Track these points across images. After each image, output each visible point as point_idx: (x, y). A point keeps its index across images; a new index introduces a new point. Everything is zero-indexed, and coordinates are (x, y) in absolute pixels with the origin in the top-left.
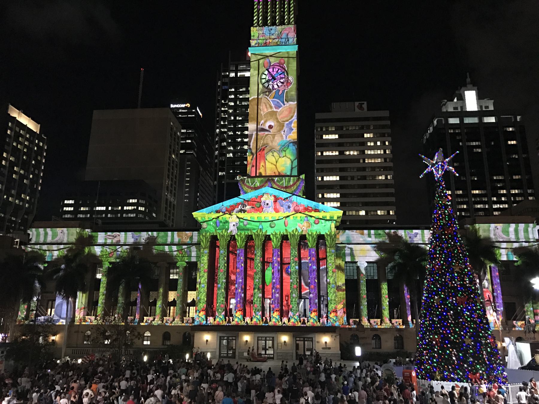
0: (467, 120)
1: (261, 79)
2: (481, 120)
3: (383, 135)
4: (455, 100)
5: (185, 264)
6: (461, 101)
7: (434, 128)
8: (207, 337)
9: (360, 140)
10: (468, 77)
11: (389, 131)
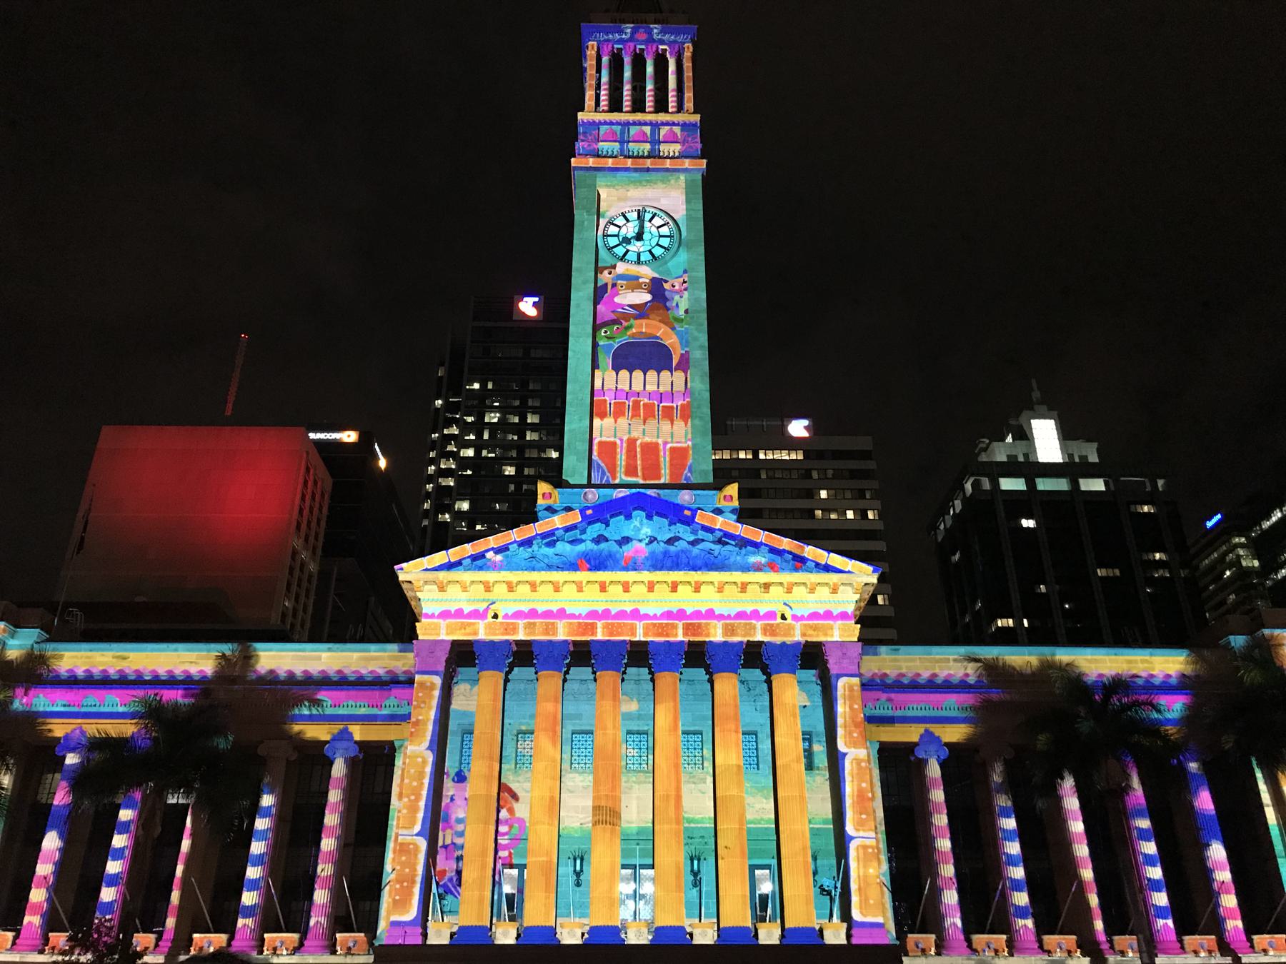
0: (1043, 484)
2: (1075, 484)
3: (861, 494)
4: (1009, 439)
6: (1024, 442)
7: (965, 501)
9: (803, 504)
11: (875, 484)
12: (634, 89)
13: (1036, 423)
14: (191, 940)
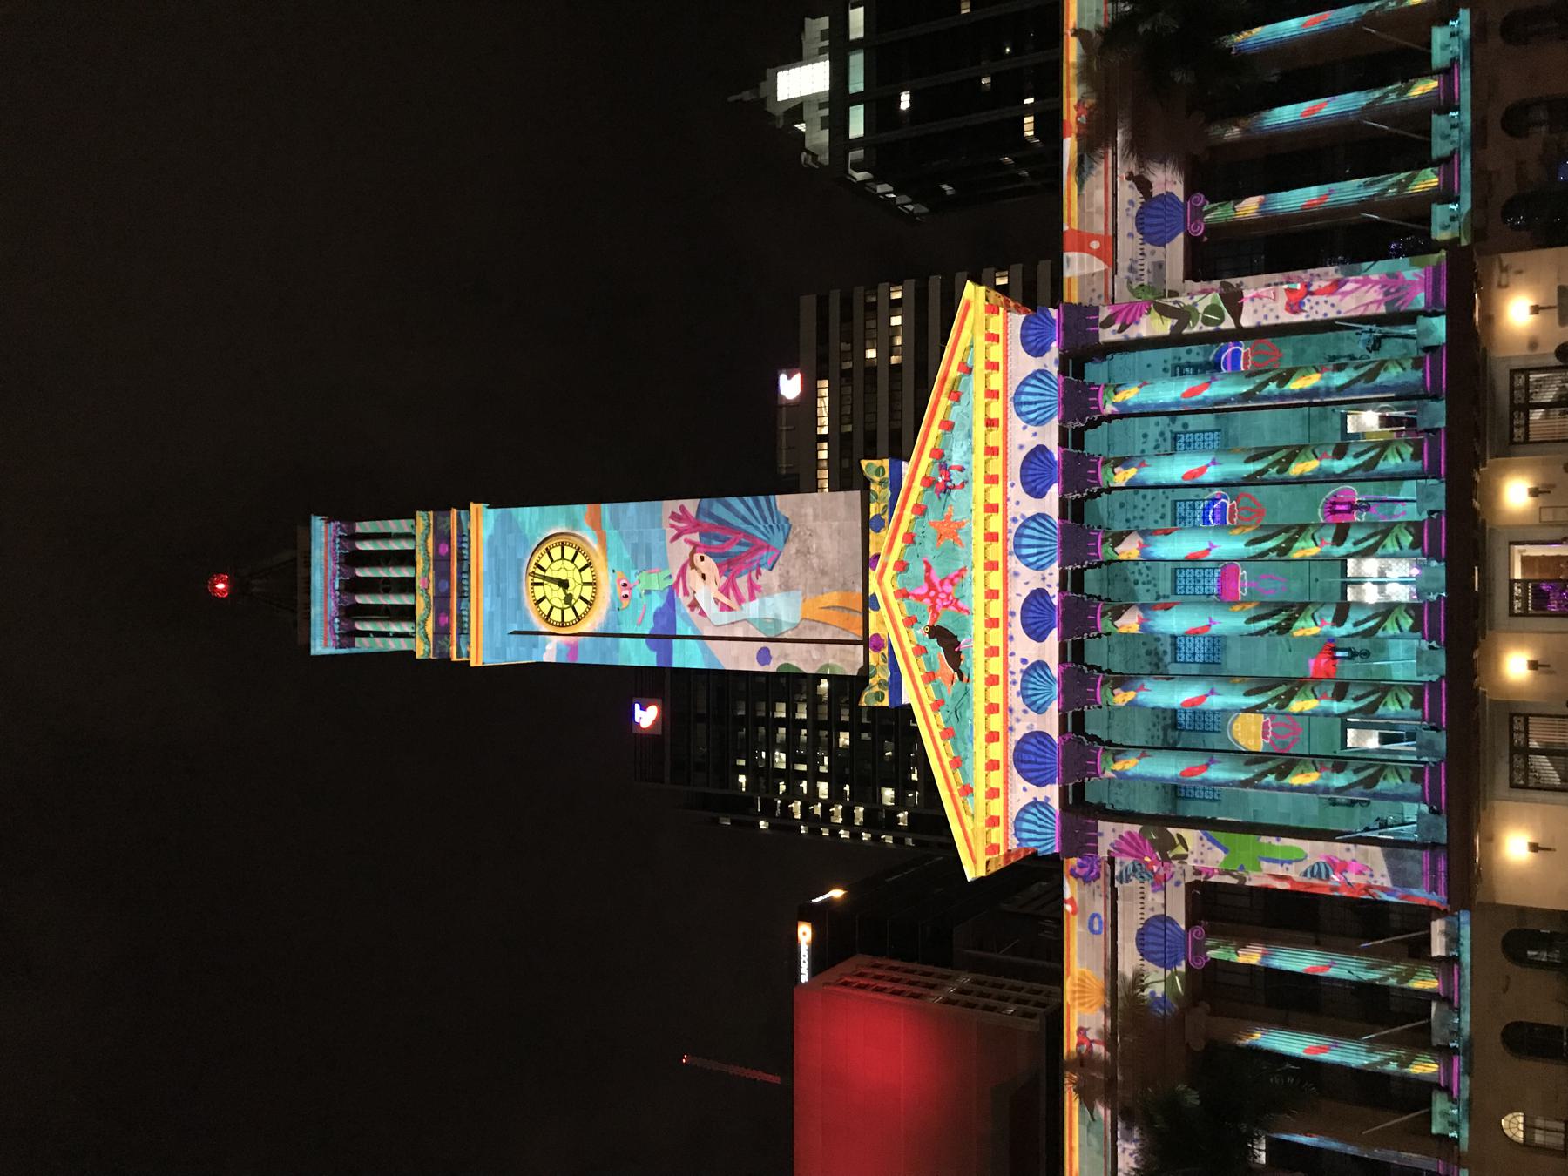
0: (857, 84)
1: (563, 624)
2: (857, 45)
3: (872, 308)
4: (802, 127)
5: (1200, 930)
7: (878, 179)
8: (1515, 846)
10: (738, 97)
11: (859, 291)
12: (387, 591)
13: (781, 97)
14: (1442, 1138)
